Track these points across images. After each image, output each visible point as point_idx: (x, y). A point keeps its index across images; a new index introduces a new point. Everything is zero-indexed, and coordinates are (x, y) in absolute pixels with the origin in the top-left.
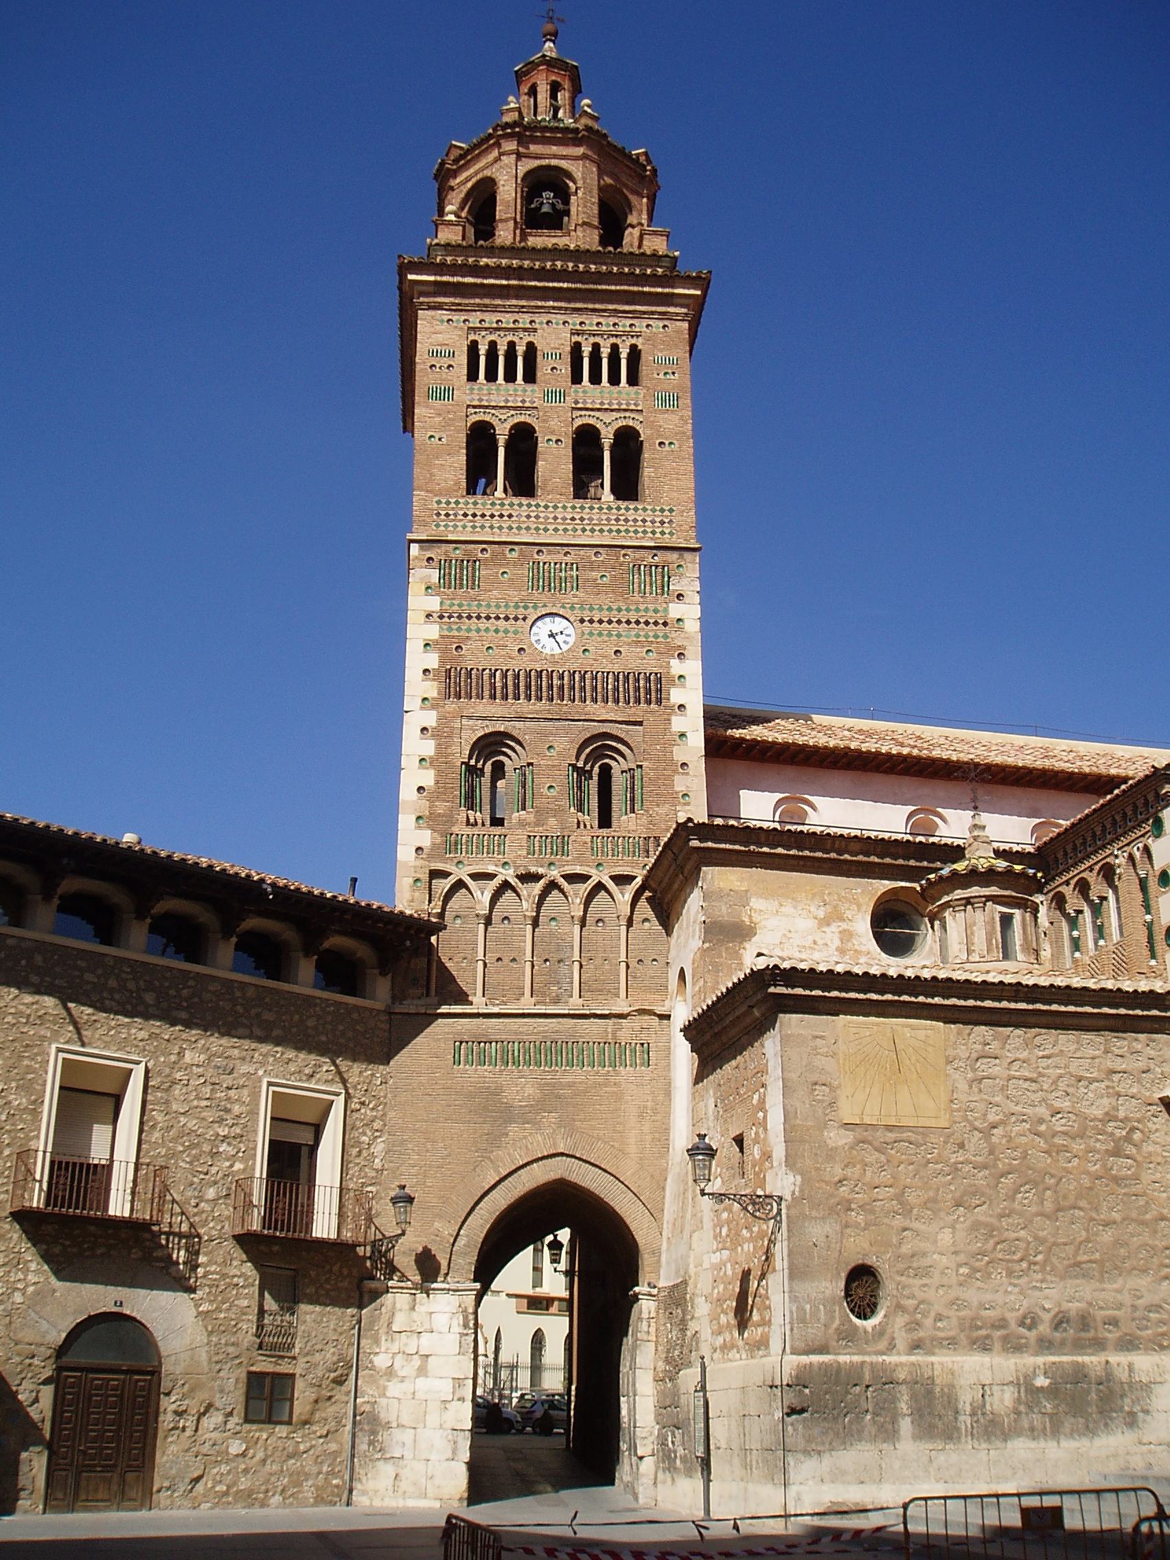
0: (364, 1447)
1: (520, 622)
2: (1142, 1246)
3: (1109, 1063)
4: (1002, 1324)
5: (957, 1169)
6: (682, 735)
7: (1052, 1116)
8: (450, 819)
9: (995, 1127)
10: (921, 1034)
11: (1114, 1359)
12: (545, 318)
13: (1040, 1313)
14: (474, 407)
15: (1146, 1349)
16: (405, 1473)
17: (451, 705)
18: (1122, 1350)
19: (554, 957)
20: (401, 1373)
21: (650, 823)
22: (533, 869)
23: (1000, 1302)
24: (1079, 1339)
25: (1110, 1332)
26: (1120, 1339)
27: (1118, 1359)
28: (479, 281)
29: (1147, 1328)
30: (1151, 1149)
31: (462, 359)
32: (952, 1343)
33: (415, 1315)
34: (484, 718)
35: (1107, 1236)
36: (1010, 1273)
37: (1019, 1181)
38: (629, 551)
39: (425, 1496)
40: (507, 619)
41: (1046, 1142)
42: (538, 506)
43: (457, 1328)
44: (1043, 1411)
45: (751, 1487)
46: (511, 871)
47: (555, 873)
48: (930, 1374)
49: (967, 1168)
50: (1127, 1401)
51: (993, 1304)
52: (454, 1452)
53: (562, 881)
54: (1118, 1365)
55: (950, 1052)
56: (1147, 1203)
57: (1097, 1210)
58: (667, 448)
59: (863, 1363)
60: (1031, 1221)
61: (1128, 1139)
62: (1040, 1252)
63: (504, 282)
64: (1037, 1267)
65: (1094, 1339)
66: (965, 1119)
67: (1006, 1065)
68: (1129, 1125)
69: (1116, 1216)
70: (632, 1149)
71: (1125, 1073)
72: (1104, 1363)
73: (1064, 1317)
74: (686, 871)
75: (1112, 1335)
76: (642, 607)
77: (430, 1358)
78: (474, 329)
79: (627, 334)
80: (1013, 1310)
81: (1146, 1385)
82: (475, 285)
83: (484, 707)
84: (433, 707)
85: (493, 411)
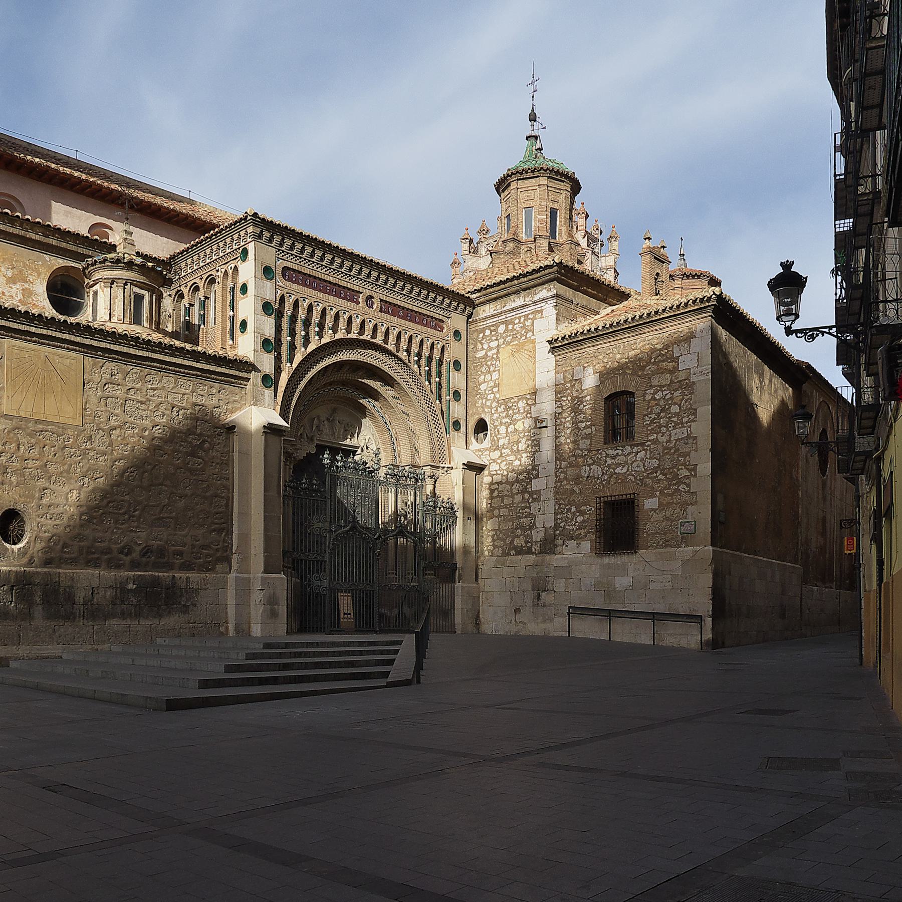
2: (201, 510)
4: (108, 551)
25: (177, 559)
32: (73, 562)
35: (181, 504)
36: (116, 522)
48: (57, 580)
59: (10, 571)
64: (135, 519)
73: (149, 549)
75: (178, 561)
80: (116, 543)
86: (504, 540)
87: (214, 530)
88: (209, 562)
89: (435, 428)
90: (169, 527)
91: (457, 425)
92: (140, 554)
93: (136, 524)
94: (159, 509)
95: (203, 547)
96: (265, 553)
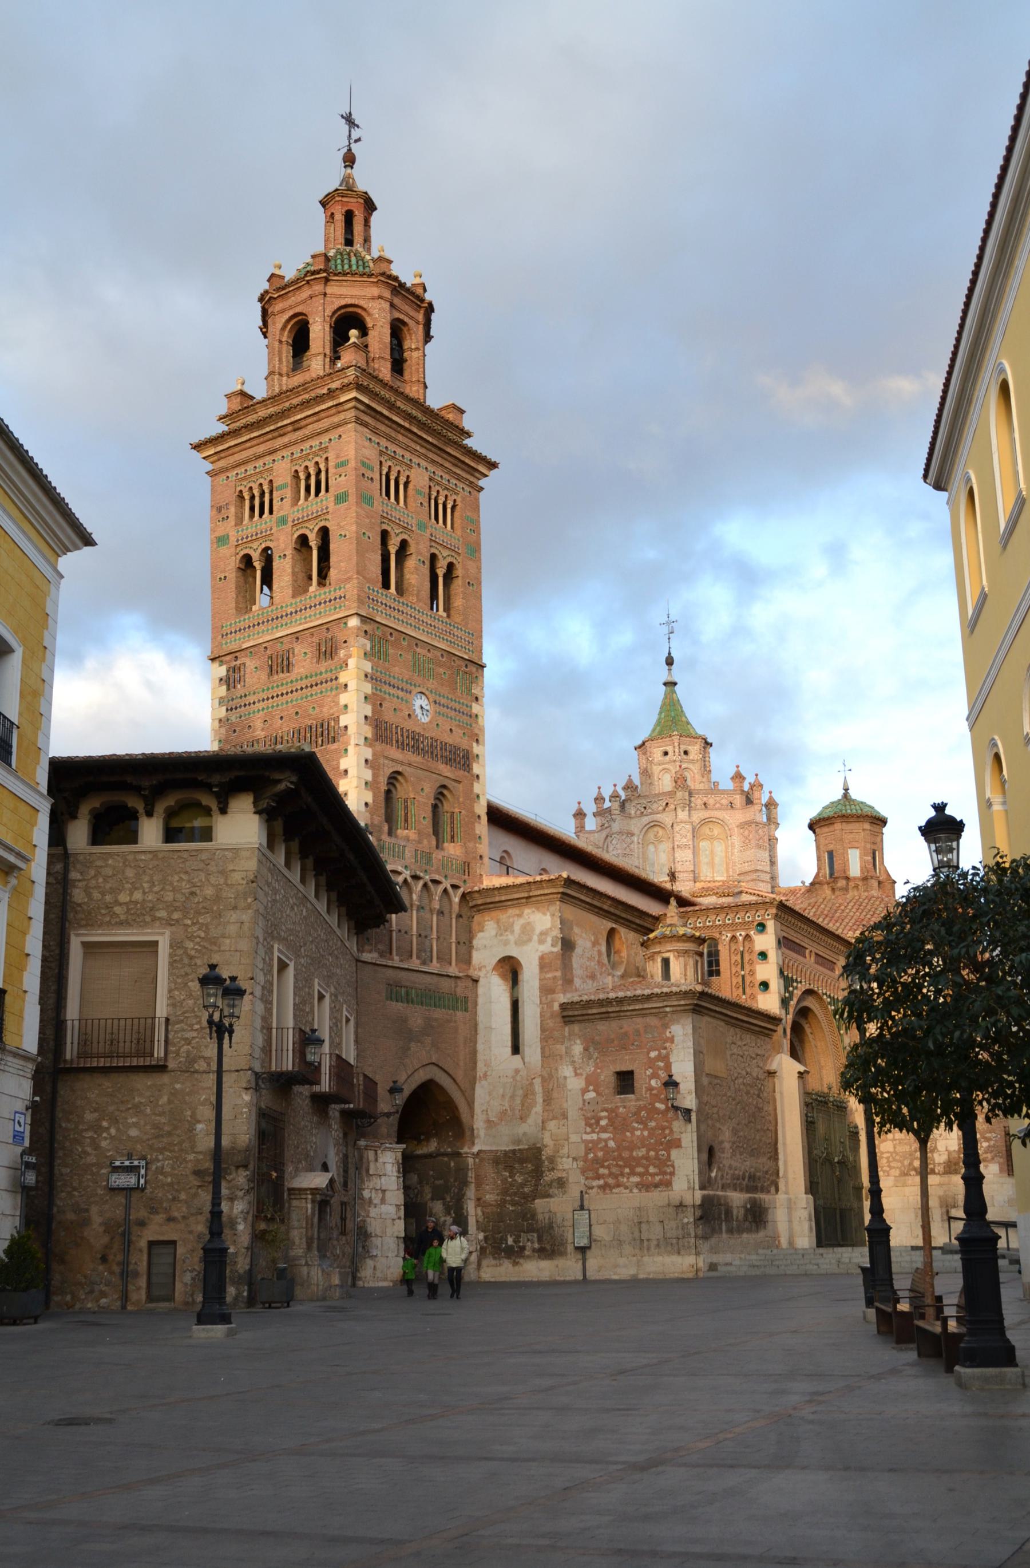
0: (360, 1249)
1: (408, 694)
12: (416, 460)
16: (378, 1266)
17: (379, 746)
19: (423, 934)
20: (377, 1201)
21: (466, 852)
22: (418, 873)
31: (377, 476)
33: (378, 1164)
34: (393, 760)
38: (456, 658)
39: (385, 1279)
40: (402, 690)
42: (415, 609)
43: (395, 1174)
45: (646, 1259)
46: (408, 872)
47: (427, 877)
52: (398, 1250)
53: (430, 883)
58: (471, 588)
70: (461, 1064)
74: (531, 900)
76: (461, 701)
77: (387, 1193)
82: (387, 418)
84: (371, 746)
85: (392, 525)
86: (901, 1162)
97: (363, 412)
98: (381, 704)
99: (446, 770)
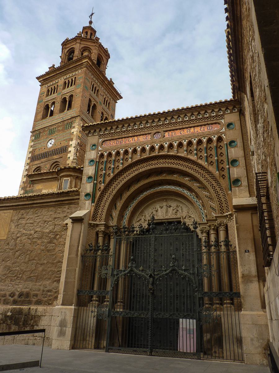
2: (51, 271)
3: (55, 216)
4: (4, 296)
5: (5, 250)
6: (69, 158)
7: (35, 233)
8: (26, 187)
9: (18, 238)
10: (6, 214)
11: (32, 307)
13: (16, 293)
14: (46, 102)
15: (44, 304)
17: (31, 164)
18: (36, 305)
23: (6, 289)
24: (25, 301)
25: (34, 298)
26: (37, 301)
27: (33, 307)
28: (49, 76)
29: (46, 297)
30: (61, 240)
31: (46, 93)
35: (41, 269)
36: (11, 280)
37: (21, 253)
38: (66, 121)
41: (31, 241)
44: (7, 323)
49: (8, 250)
50: (32, 321)
51: (4, 290)
54: (33, 309)
55: (13, 218)
56: (56, 257)
57: (39, 260)
60: (21, 265)
61: (55, 238)
62: (21, 274)
63: (53, 75)
64: (19, 278)
65: (29, 300)
66: (11, 236)
67: (26, 220)
68: (56, 233)
69: (45, 262)
71: (59, 218)
72: (28, 309)
73: (22, 294)
78: (49, 87)
79: (74, 75)
80: (9, 291)
81: (39, 316)
83: (36, 162)
87: (55, 281)
88: (50, 300)
89: (220, 190)
90: (33, 281)
91: (236, 181)
92: (18, 296)
93: (19, 281)
94: (30, 272)
95: (49, 291)
96: (63, 292)
97: (44, 82)
98: (35, 151)
99: (55, 157)
